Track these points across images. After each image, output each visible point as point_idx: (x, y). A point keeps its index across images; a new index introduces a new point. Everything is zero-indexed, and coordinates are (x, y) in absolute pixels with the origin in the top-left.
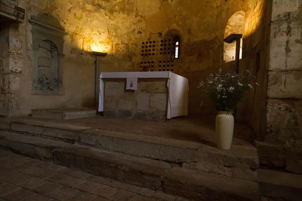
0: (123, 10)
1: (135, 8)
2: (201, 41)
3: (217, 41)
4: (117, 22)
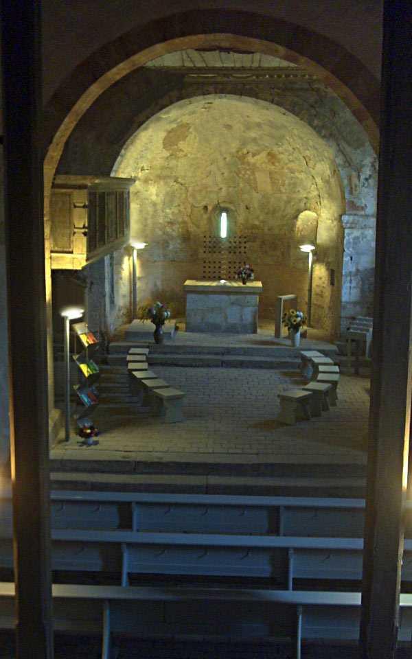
0: (160, 177)
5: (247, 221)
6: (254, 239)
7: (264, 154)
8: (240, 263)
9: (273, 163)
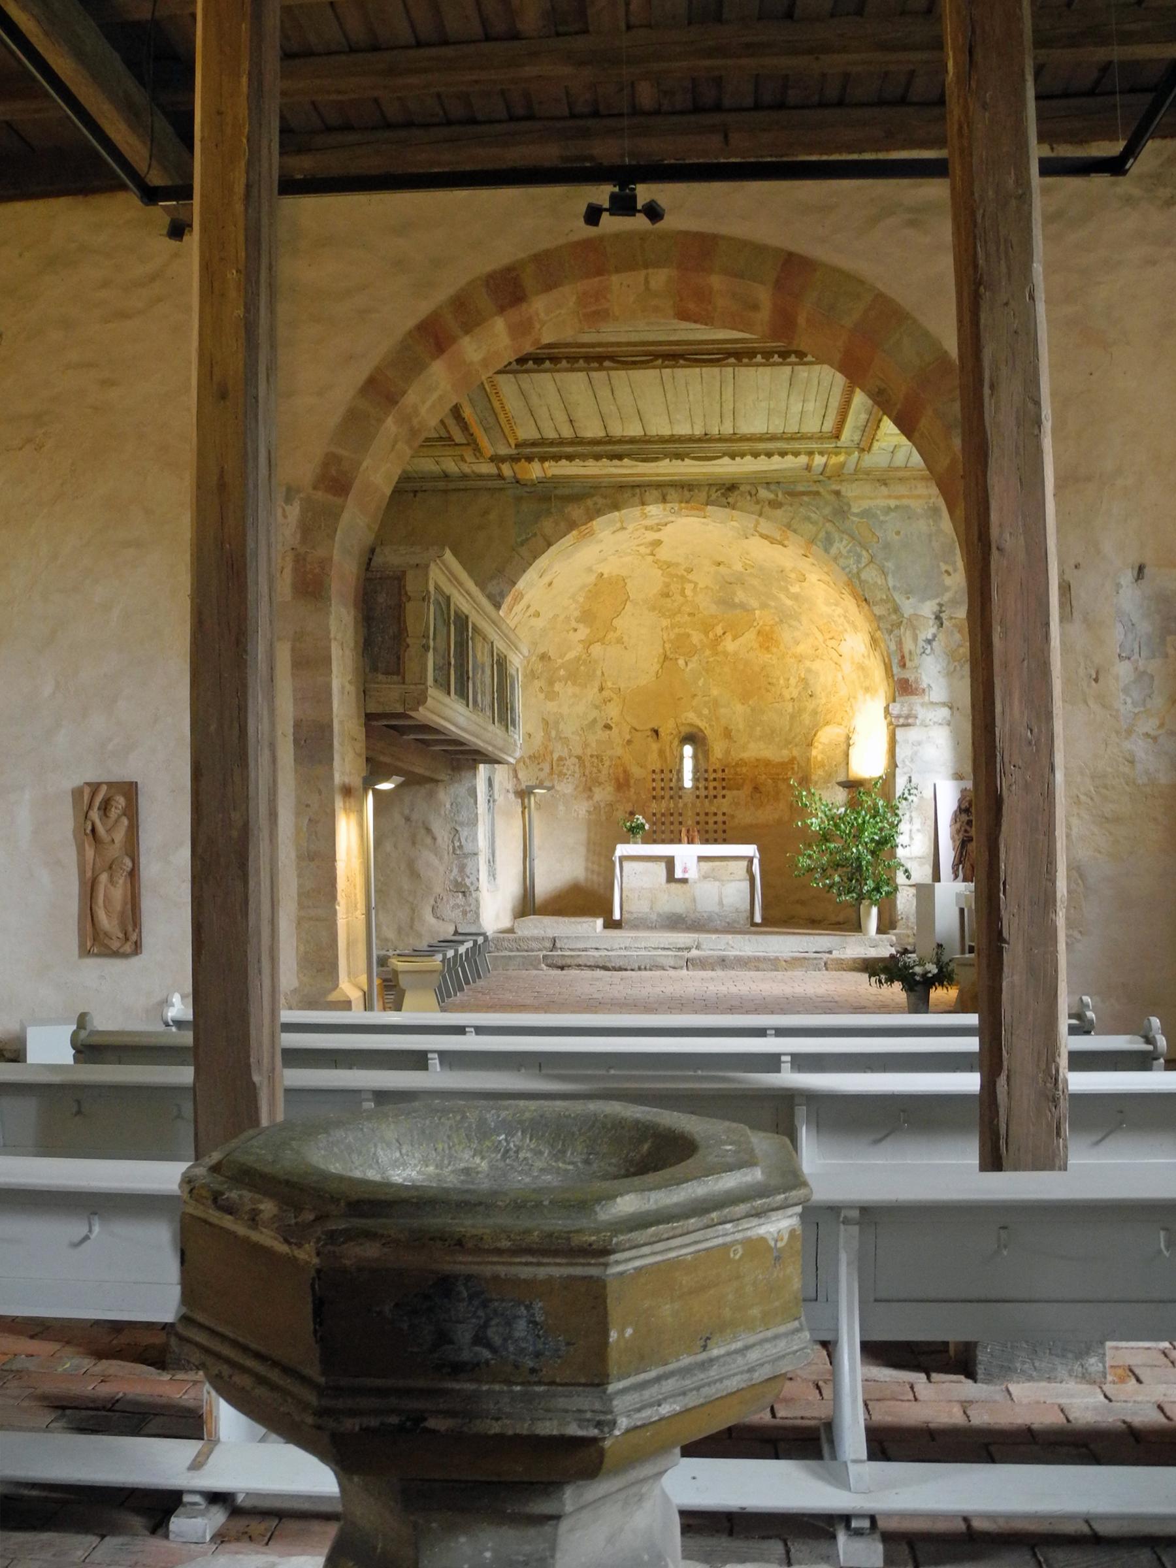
1: (599, 673)
2: (757, 760)
3: (796, 767)
5: (728, 752)
8: (715, 797)
9: (767, 648)
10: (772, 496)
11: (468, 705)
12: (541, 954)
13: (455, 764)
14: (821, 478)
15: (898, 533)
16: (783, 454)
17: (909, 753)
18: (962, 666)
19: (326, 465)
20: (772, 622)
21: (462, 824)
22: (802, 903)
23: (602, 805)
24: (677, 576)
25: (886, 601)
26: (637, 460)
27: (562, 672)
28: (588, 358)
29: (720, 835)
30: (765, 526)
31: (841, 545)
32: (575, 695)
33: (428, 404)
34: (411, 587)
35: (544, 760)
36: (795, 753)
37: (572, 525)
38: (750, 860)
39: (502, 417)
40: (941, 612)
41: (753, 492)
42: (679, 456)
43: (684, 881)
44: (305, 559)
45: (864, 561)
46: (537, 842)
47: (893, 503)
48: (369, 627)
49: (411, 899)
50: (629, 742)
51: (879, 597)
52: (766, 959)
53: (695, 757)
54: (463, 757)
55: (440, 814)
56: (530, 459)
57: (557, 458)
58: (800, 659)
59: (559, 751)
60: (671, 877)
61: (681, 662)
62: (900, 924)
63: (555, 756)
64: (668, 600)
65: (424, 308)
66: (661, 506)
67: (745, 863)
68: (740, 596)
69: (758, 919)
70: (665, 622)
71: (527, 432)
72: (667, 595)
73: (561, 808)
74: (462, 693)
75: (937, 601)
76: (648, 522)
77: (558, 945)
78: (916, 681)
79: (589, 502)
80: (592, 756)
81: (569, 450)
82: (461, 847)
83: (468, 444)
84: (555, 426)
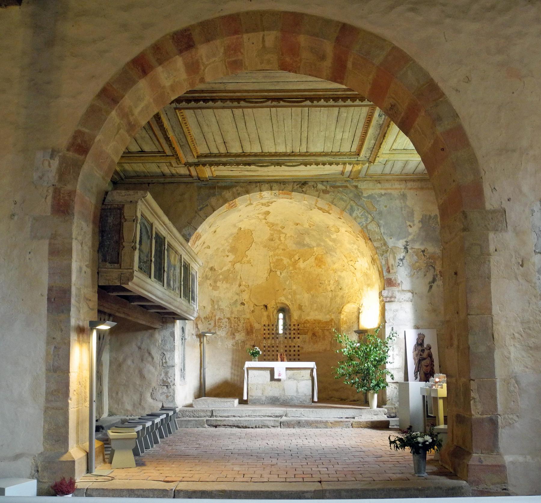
1: (239, 277)
2: (315, 320)
3: (333, 324)
4: (220, 293)
5: (300, 317)
6: (306, 333)
7: (312, 260)
8: (294, 338)
9: (320, 266)
10: (324, 188)
11: (163, 286)
12: (205, 419)
13: (164, 320)
14: (348, 179)
15: (386, 206)
16: (331, 164)
17: (392, 315)
18: (418, 272)
19: (75, 137)
20: (323, 253)
21: (167, 351)
22: (337, 390)
23: (240, 342)
24: (276, 230)
25: (380, 240)
26: (258, 166)
27: (221, 277)
28: (232, 100)
29: (297, 357)
30: (321, 203)
31: (357, 212)
32: (227, 288)
33: (139, 109)
34: (127, 213)
35: (211, 319)
36: (333, 317)
37: (225, 201)
38: (312, 370)
39: (189, 138)
40: (407, 245)
41: (315, 186)
42: (279, 164)
43: (279, 380)
44: (60, 192)
45: (369, 220)
46: (207, 360)
47: (383, 192)
48: (102, 236)
49: (140, 389)
50: (253, 311)
51: (377, 238)
52: (321, 422)
53: (284, 318)
54: (167, 317)
55: (156, 346)
56: (204, 165)
57: (218, 164)
58: (335, 271)
59: (219, 315)
60: (272, 378)
61: (278, 273)
62: (388, 402)
63: (217, 318)
64: (273, 242)
65: (136, 51)
66: (270, 192)
67: (309, 371)
68: (307, 240)
69: (316, 399)
70: (271, 253)
71: (202, 149)
72: (272, 240)
73: (220, 343)
74: (159, 277)
75: (405, 240)
76: (263, 201)
77: (214, 414)
78: (395, 280)
79: (234, 190)
80: (235, 318)
81: (224, 160)
82: (166, 362)
83: (173, 156)
84: (216, 147)
